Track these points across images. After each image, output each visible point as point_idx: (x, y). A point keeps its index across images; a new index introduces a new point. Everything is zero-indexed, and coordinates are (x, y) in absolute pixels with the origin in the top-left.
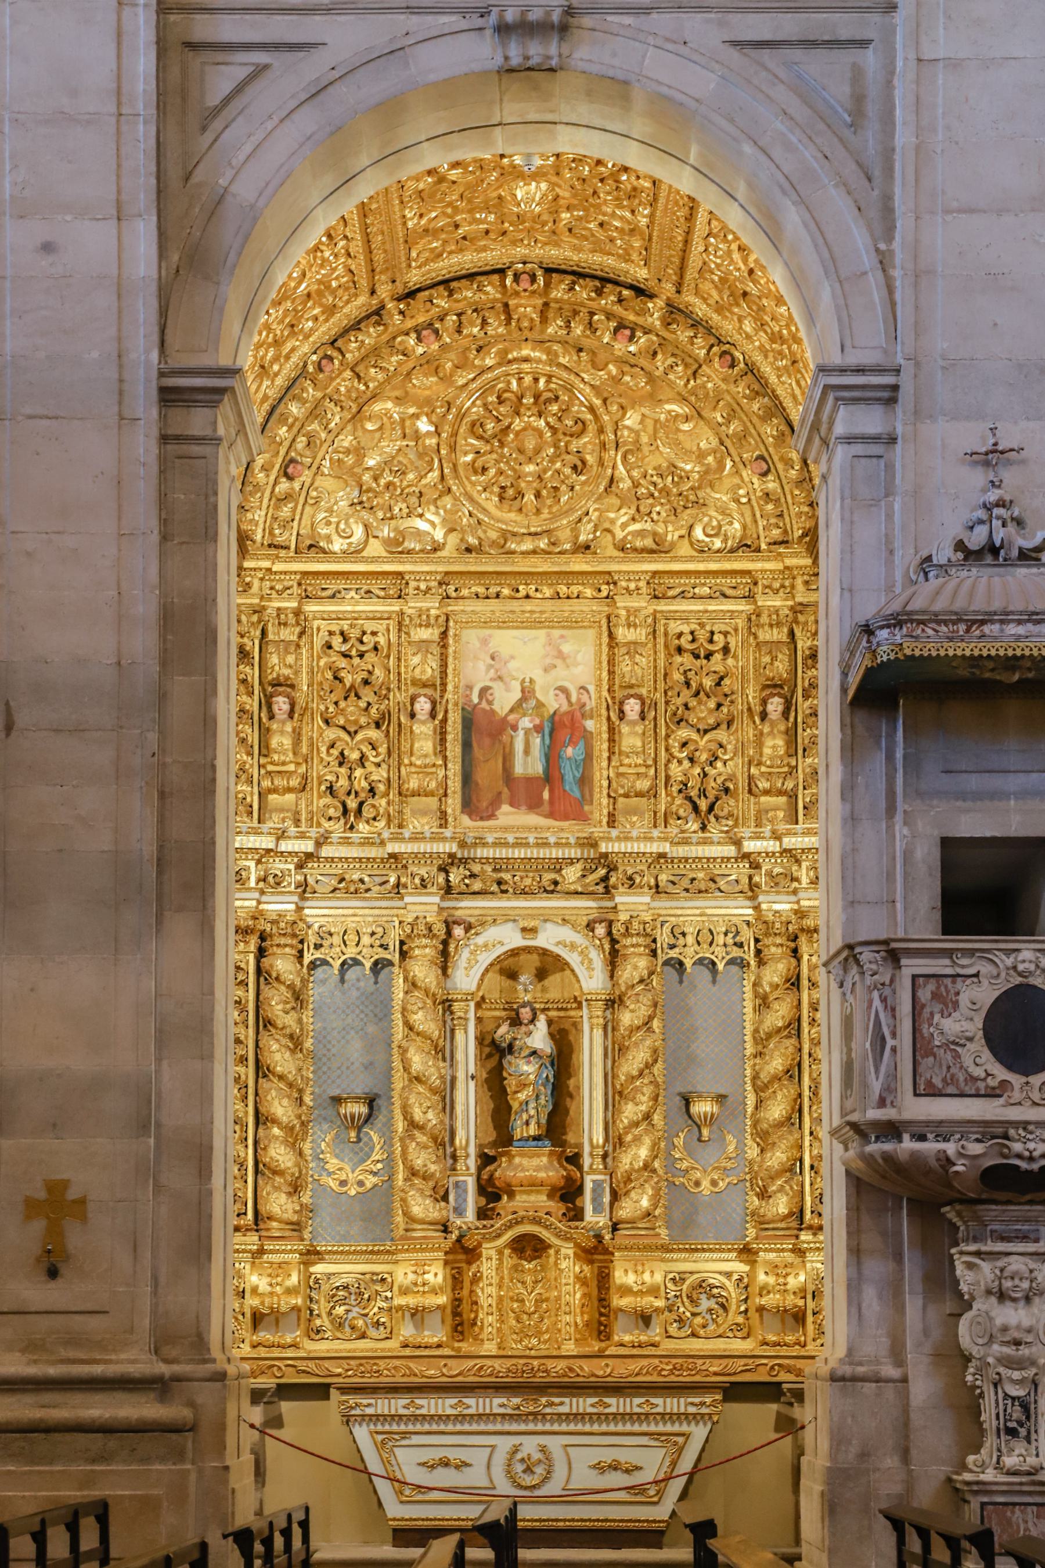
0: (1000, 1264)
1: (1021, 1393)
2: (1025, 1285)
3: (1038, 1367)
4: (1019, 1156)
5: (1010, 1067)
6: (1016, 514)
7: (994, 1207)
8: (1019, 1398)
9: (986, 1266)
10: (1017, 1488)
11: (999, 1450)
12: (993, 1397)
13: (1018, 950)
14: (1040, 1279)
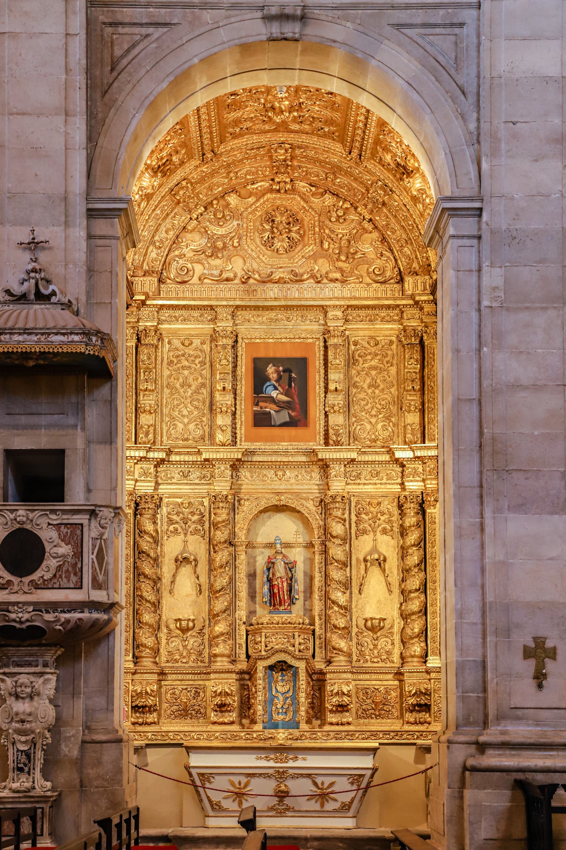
0: (15, 679)
1: (26, 748)
2: (28, 690)
3: (36, 734)
4: (14, 621)
5: (12, 573)
6: (43, 276)
7: (11, 648)
8: (25, 751)
9: (8, 680)
10: (17, 800)
11: (14, 780)
12: (12, 751)
13: (17, 510)
14: (36, 687)
